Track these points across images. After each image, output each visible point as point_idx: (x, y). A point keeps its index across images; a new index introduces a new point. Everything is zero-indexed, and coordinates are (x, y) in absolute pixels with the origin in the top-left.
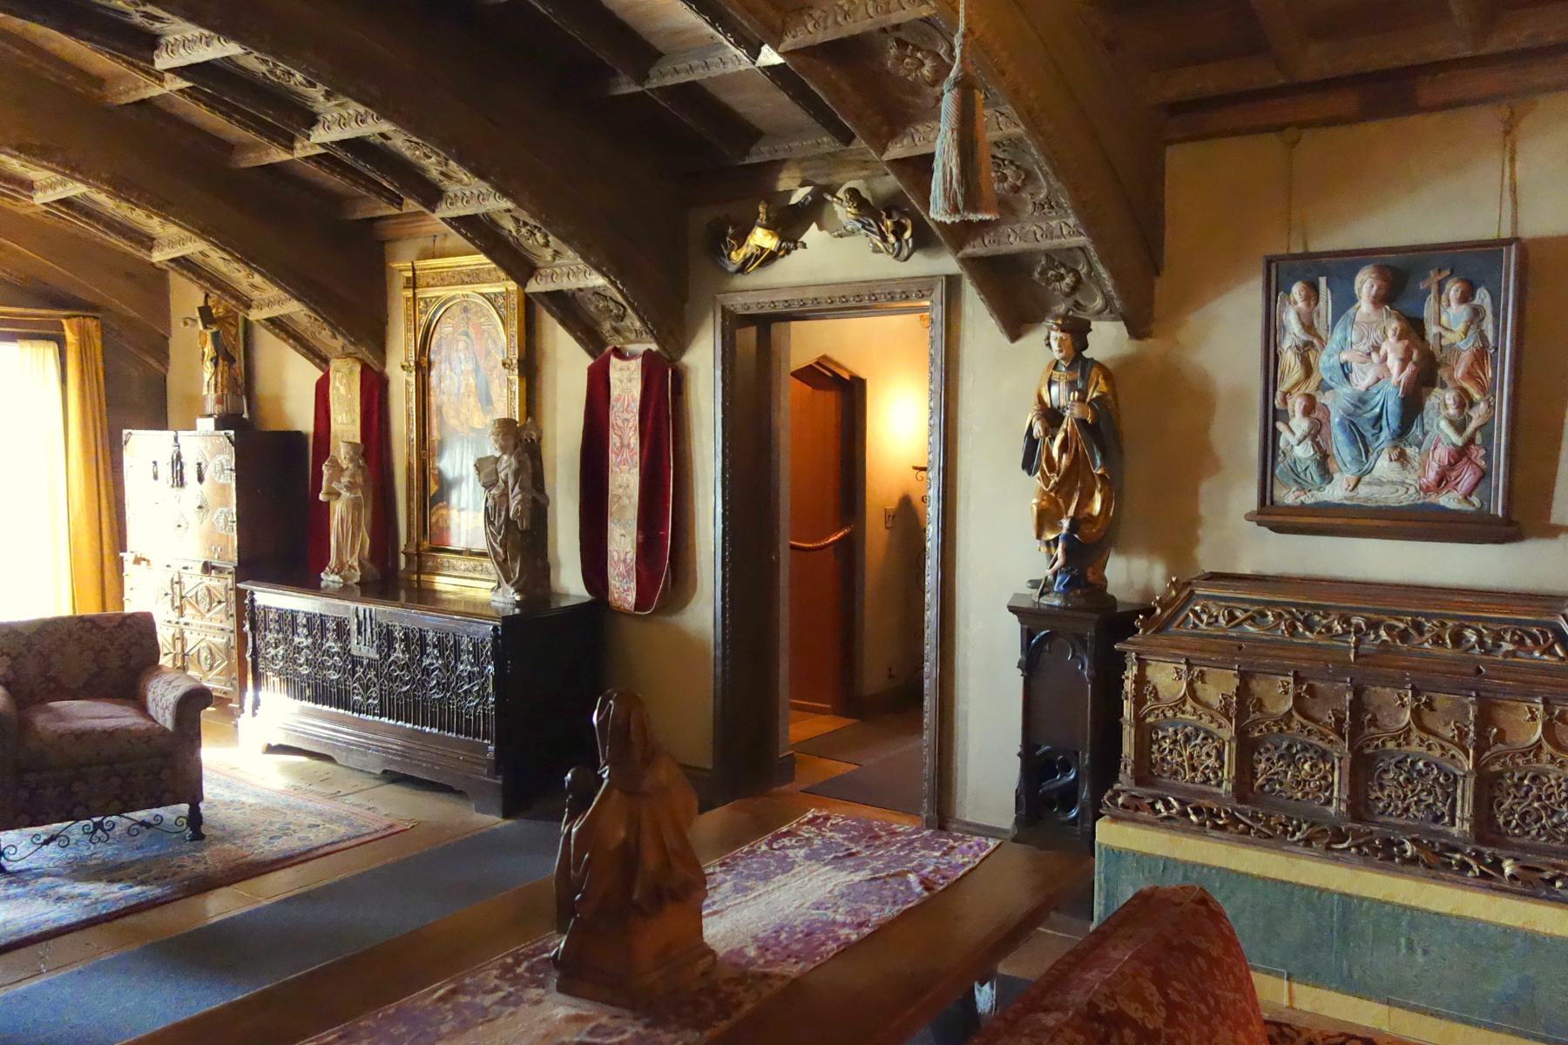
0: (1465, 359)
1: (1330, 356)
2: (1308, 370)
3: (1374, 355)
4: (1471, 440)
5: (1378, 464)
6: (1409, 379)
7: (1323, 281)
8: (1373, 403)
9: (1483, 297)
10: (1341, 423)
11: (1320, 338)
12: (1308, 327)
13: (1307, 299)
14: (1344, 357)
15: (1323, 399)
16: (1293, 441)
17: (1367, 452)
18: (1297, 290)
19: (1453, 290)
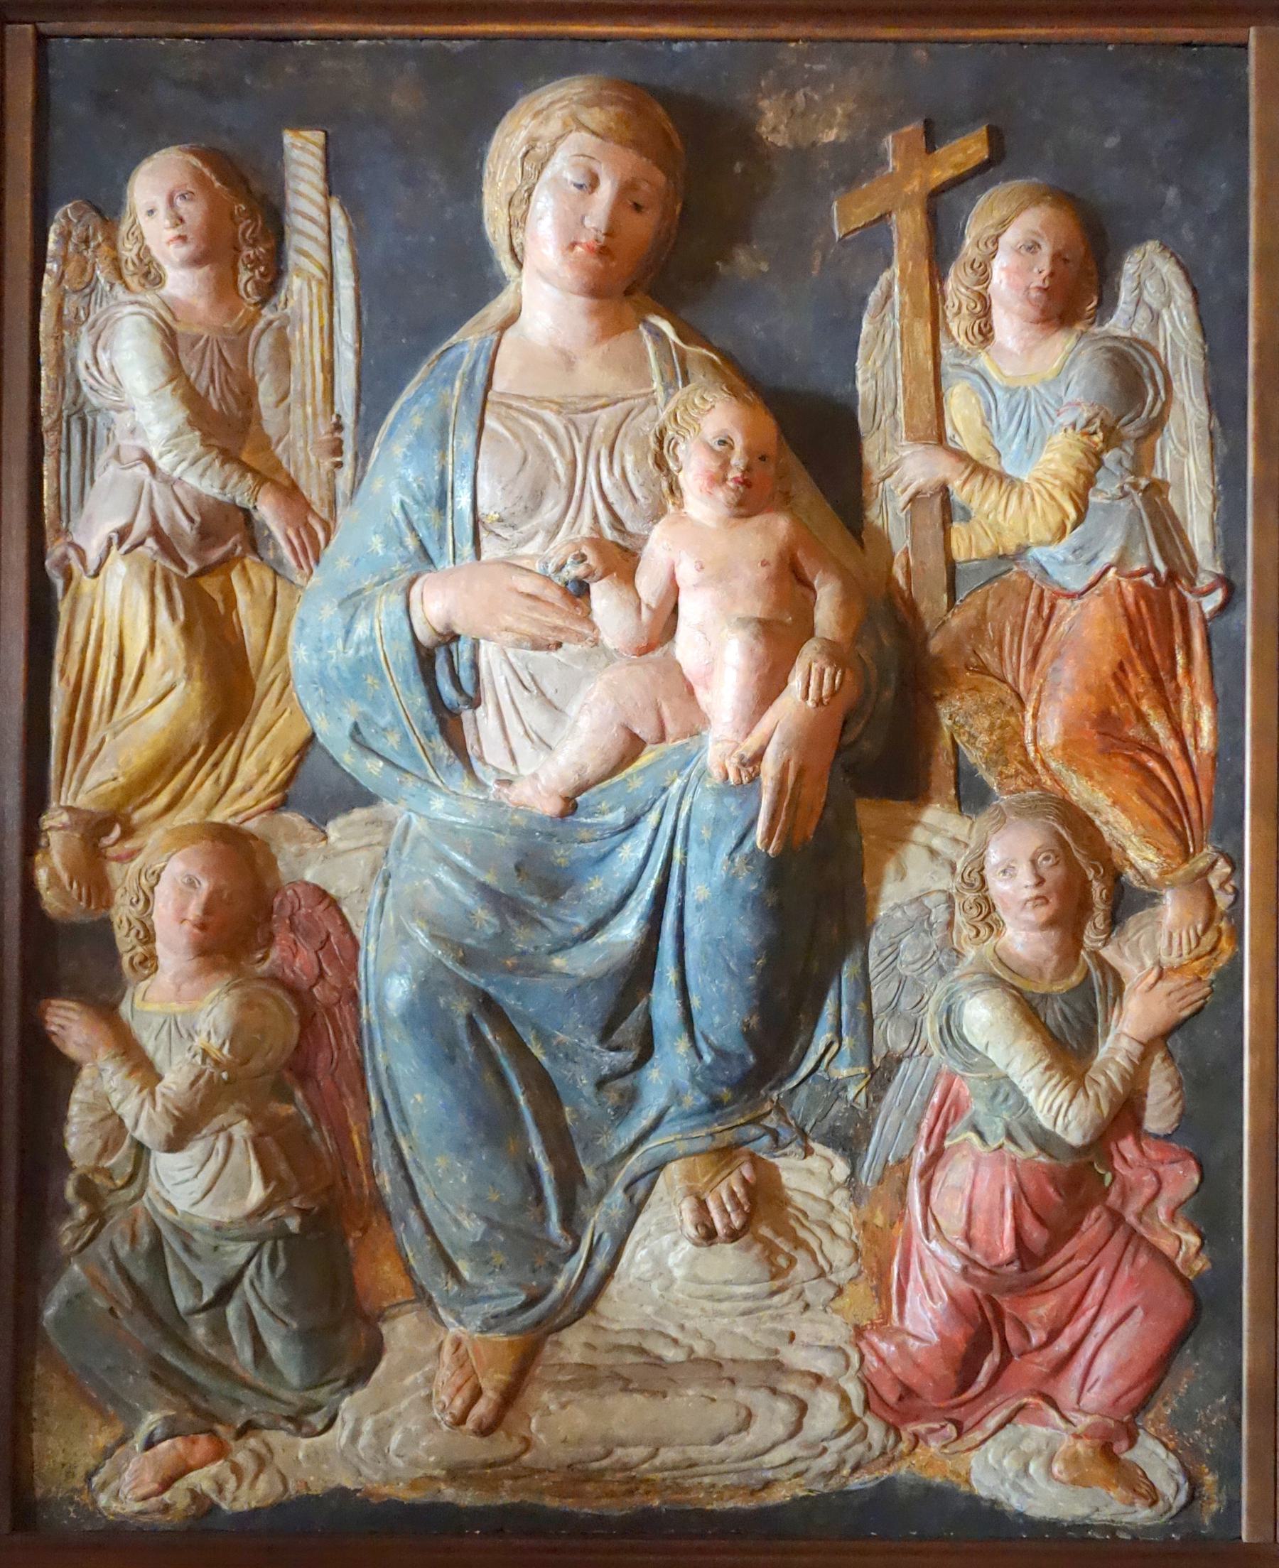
0: (1088, 630)
1: (354, 602)
2: (230, 683)
3: (603, 598)
4: (1125, 1113)
5: (636, 1259)
6: (806, 741)
7: (303, 154)
8: (600, 887)
9: (1154, 295)
10: (424, 1013)
11: (291, 492)
12: (226, 420)
13: (214, 251)
14: (435, 605)
15: (326, 859)
16: (146, 1123)
17: (570, 1181)
18: (158, 197)
19: (1011, 245)
